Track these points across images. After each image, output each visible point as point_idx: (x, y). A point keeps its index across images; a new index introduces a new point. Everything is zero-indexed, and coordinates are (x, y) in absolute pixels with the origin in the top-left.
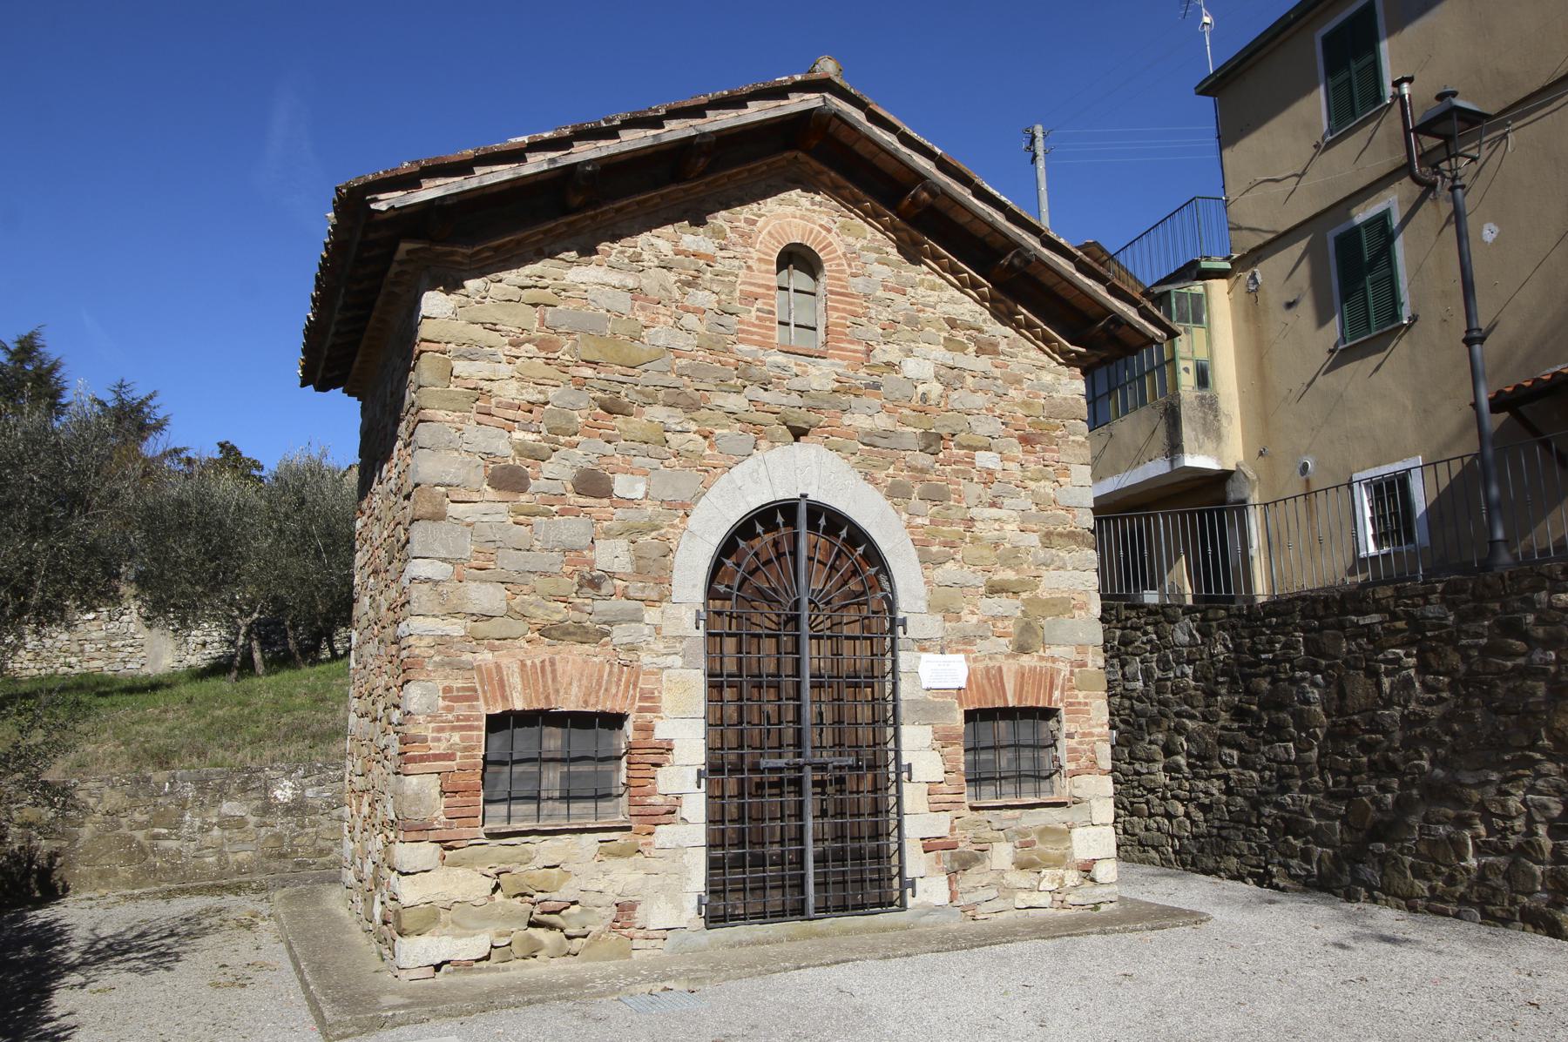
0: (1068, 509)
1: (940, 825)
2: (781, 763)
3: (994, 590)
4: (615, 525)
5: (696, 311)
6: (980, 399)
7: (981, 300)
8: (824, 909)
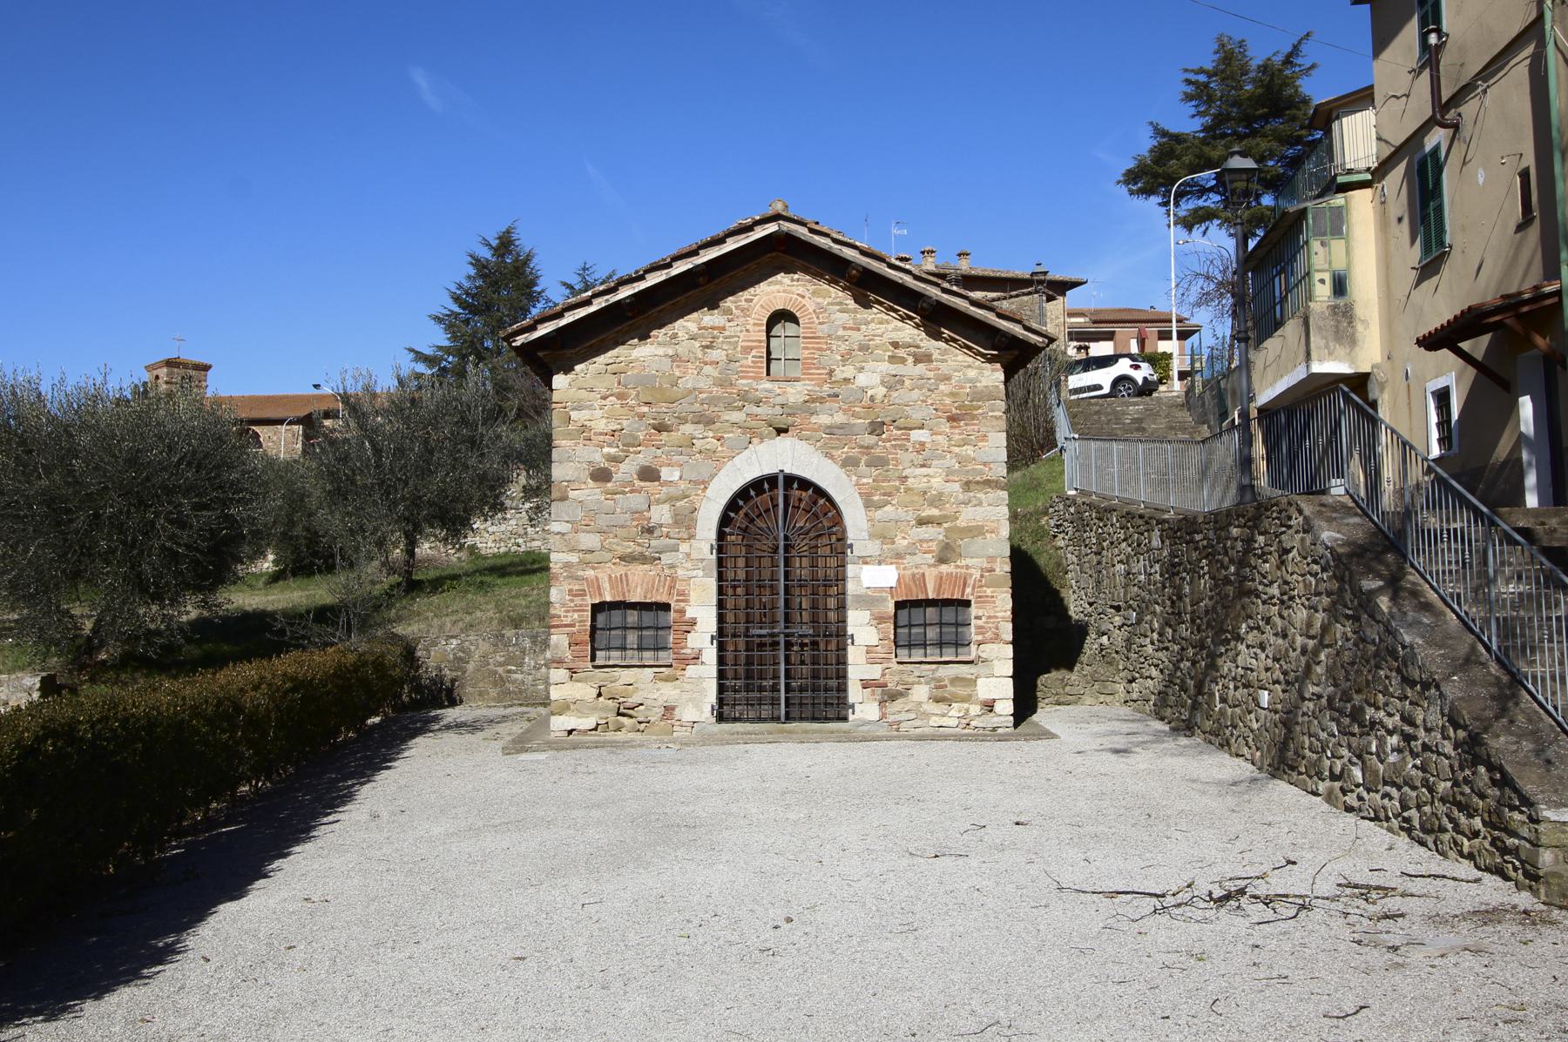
0: (985, 464)
1: (875, 672)
2: (764, 632)
3: (922, 522)
4: (662, 496)
5: (711, 363)
6: (916, 394)
7: (917, 326)
8: (788, 718)
